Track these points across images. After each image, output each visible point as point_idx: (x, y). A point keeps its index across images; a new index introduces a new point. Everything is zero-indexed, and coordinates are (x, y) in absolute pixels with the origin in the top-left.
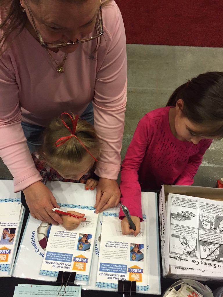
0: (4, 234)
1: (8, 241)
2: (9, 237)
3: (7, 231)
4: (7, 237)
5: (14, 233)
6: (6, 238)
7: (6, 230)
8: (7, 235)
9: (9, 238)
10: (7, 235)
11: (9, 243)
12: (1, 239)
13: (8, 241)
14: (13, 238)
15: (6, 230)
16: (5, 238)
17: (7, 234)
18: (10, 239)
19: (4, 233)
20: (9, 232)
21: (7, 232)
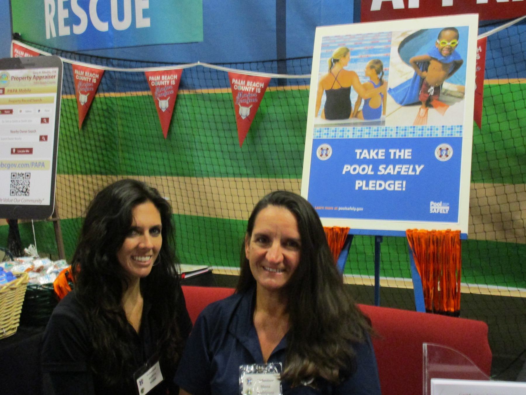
0: (381, 82)
1: (355, 53)
2: (353, 74)
3: (367, 102)
4: (360, 69)
5: (330, 93)
6: (368, 64)
7: (372, 105)
8: (364, 81)
9: (349, 67)
10: (364, 81)
11: (348, 44)
12: (388, 58)
13: (355, 53)
14: (332, 66)
15: (372, 105)
16: (372, 67)
17: (365, 87)
18: (342, 61)
19: (380, 89)
20: (354, 97)
21: (367, 96)
